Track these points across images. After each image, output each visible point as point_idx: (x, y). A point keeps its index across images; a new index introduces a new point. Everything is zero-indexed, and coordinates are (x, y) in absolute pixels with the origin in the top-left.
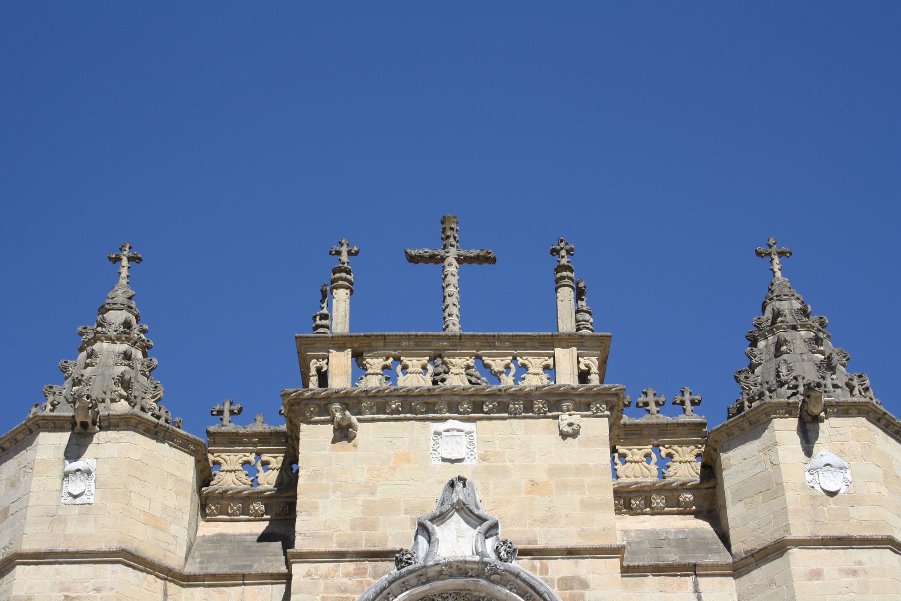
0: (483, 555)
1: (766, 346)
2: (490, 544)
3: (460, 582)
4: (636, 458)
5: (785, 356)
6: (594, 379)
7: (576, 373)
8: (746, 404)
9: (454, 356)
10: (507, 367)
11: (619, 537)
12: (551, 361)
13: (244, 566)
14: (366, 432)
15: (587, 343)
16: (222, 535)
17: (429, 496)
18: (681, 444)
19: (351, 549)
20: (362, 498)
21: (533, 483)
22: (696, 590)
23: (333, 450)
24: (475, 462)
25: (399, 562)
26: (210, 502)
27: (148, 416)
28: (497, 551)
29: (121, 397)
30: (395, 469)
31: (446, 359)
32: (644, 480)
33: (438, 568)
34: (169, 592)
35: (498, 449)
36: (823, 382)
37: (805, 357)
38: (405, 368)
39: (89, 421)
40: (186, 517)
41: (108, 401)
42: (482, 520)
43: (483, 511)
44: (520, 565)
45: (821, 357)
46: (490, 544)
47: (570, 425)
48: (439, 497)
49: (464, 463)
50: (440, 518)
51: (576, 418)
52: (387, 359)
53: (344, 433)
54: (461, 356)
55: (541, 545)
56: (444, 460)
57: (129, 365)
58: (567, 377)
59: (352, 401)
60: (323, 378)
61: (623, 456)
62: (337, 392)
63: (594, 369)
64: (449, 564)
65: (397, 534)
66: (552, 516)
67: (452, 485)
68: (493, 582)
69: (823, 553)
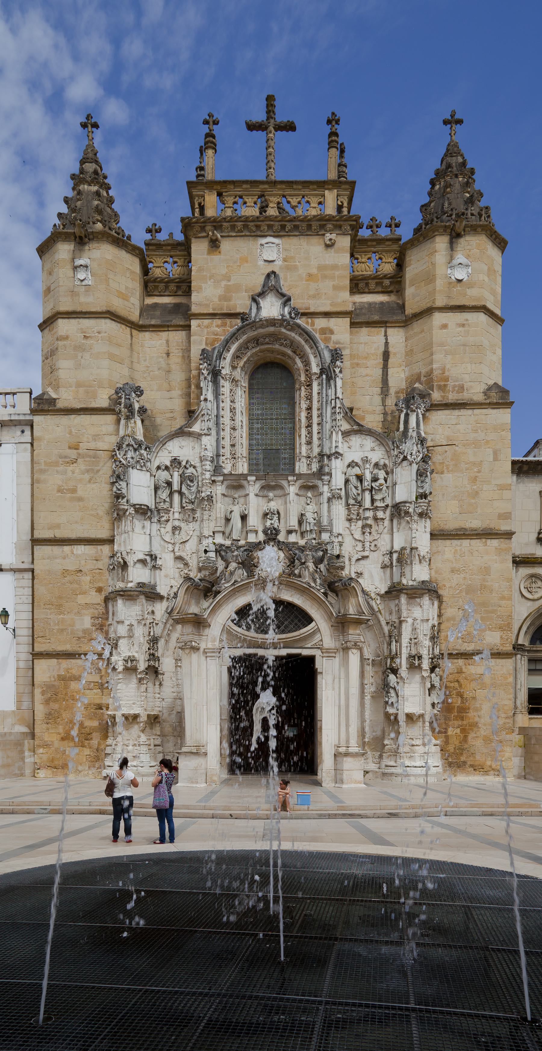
0: (283, 315)
1: (440, 188)
2: (287, 310)
3: (272, 329)
4: (363, 260)
5: (448, 195)
6: (345, 210)
7: (336, 207)
8: (424, 226)
9: (271, 195)
10: (299, 203)
11: (351, 306)
12: (322, 200)
13: (168, 321)
14: (226, 245)
15: (343, 187)
16: (156, 303)
17: (258, 282)
18: (387, 251)
19: (219, 312)
20: (224, 283)
21: (310, 275)
22: (386, 335)
23: (209, 253)
24: (280, 263)
25: (243, 320)
26: (150, 285)
27: (113, 233)
28: (290, 313)
29: (98, 221)
30: (240, 266)
31: (267, 197)
32: (364, 273)
33: (261, 323)
34: (133, 334)
35: (292, 255)
36: (466, 212)
37: (459, 196)
38: (245, 203)
39: (83, 236)
40: (138, 294)
41: (91, 223)
42: (283, 295)
43: (284, 290)
44: (300, 321)
45: (468, 195)
46: (287, 310)
47: (330, 240)
48: (262, 283)
49: (275, 263)
50: (262, 294)
51: (333, 236)
52: (236, 197)
53: (214, 244)
54: (274, 195)
55: (312, 310)
56: (265, 261)
57: (99, 200)
58: (330, 209)
59: (217, 224)
60: (202, 208)
61: (357, 259)
62: (210, 218)
63: (345, 204)
64: (267, 320)
65: (241, 303)
66: (318, 294)
67: (268, 276)
68: (288, 330)
69: (450, 315)
